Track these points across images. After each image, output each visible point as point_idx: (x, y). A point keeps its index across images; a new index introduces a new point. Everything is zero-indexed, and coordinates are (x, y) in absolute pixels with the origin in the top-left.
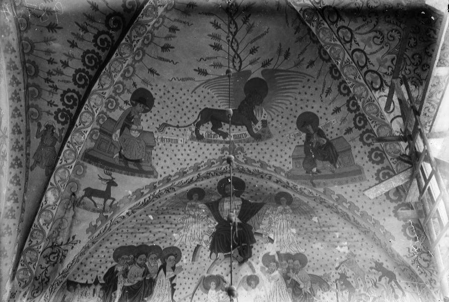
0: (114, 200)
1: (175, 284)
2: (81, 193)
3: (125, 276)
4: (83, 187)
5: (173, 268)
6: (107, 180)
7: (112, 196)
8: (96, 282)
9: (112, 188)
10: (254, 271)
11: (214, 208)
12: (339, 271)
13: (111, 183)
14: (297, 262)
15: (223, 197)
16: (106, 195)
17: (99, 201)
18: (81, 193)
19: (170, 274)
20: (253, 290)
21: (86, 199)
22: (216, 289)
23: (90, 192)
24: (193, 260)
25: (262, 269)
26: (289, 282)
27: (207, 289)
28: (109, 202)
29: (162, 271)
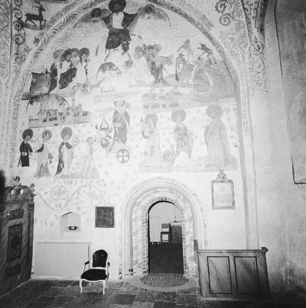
0: (46, 21)
1: (87, 70)
2: (24, 19)
3: (61, 67)
4: (24, 14)
5: (86, 61)
6: (39, 7)
7: (44, 19)
8: (47, 72)
9: (43, 13)
10: (130, 58)
11: (107, 21)
12: (179, 52)
13: (41, 9)
14: (155, 50)
15: (113, 13)
16: (40, 18)
17: (37, 23)
18: (24, 19)
19: (84, 64)
20: (129, 69)
21: (28, 22)
22: (110, 70)
23: (30, 17)
24: (97, 54)
25: (135, 56)
26: (149, 62)
27: (104, 71)
28: (43, 23)
29: (80, 63)
